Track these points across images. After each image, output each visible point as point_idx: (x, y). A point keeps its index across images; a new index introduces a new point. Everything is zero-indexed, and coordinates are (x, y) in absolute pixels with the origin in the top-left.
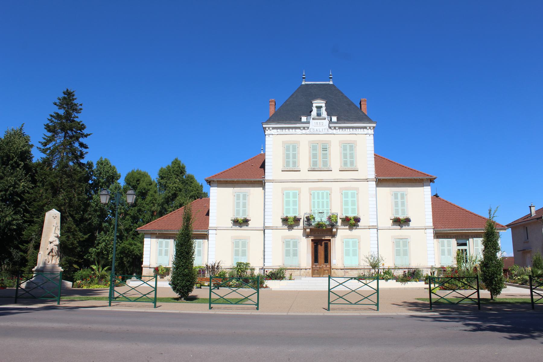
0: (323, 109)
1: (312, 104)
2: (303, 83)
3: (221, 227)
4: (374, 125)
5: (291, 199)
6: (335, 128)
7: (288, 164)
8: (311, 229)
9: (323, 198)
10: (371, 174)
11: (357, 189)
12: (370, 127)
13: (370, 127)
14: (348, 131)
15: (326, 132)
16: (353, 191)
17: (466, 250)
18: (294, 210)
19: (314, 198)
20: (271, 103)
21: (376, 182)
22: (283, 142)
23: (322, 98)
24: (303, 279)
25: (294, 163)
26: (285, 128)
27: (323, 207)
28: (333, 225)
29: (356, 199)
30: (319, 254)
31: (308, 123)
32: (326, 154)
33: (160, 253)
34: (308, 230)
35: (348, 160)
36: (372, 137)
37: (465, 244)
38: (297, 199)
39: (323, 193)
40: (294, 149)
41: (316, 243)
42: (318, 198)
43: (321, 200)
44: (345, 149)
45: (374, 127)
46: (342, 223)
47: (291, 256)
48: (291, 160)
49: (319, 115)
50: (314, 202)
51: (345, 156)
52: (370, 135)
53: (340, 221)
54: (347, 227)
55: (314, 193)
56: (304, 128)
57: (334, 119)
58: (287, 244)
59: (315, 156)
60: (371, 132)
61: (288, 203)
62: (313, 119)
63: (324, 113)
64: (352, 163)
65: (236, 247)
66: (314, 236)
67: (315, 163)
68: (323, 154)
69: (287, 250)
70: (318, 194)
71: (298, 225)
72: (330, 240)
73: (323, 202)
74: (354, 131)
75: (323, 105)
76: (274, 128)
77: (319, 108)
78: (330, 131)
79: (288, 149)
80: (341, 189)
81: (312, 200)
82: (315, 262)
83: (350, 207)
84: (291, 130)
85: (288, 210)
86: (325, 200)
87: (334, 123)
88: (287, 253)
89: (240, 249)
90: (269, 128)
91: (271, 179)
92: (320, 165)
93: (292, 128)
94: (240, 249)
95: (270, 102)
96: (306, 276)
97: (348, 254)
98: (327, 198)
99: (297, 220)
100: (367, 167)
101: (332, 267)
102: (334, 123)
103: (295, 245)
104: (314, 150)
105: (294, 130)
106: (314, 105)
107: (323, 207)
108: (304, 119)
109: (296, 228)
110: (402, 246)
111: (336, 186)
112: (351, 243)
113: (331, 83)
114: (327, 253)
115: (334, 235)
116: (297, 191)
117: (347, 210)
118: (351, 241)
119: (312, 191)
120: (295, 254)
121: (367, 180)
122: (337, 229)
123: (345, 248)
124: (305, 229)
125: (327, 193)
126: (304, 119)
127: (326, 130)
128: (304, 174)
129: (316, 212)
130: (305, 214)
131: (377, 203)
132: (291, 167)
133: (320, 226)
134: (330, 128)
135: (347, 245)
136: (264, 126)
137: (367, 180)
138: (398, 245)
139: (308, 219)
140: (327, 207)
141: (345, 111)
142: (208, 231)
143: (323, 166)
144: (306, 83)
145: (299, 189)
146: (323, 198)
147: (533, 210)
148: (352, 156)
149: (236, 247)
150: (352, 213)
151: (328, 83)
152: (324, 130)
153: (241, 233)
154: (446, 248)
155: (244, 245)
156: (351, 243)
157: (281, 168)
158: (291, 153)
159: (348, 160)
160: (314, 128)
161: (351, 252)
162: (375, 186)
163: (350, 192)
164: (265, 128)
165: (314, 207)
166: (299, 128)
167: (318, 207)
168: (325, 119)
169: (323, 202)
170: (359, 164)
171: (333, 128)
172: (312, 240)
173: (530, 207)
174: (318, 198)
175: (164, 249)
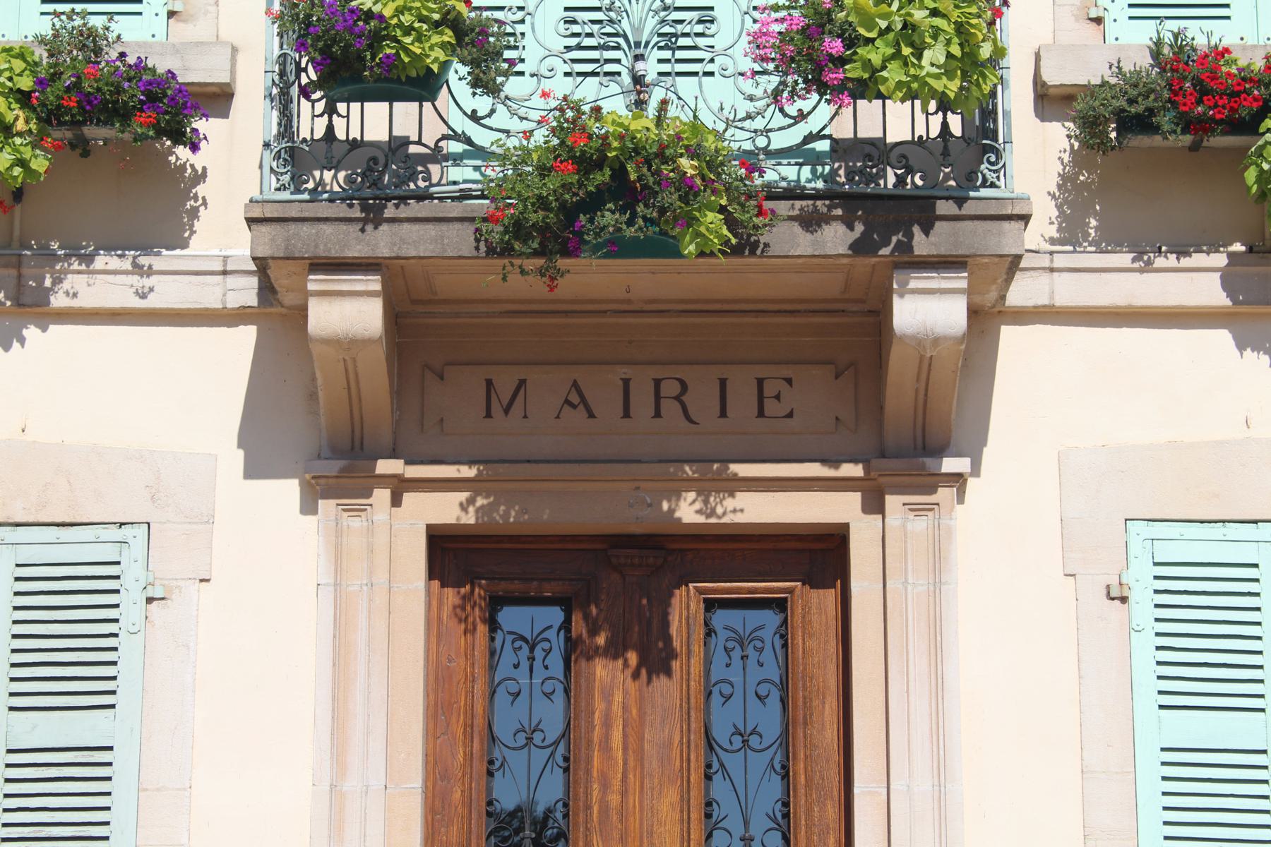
28: (902, 205)
34: (349, 313)
46: (1074, 197)
53: (1035, 157)
54: (1199, 281)
66: (497, 468)
71: (159, 218)
72: (823, 555)
109: (102, 282)
115: (911, 435)
122: (986, 317)
124: (276, 304)
133: (606, 188)
172: (448, 553)
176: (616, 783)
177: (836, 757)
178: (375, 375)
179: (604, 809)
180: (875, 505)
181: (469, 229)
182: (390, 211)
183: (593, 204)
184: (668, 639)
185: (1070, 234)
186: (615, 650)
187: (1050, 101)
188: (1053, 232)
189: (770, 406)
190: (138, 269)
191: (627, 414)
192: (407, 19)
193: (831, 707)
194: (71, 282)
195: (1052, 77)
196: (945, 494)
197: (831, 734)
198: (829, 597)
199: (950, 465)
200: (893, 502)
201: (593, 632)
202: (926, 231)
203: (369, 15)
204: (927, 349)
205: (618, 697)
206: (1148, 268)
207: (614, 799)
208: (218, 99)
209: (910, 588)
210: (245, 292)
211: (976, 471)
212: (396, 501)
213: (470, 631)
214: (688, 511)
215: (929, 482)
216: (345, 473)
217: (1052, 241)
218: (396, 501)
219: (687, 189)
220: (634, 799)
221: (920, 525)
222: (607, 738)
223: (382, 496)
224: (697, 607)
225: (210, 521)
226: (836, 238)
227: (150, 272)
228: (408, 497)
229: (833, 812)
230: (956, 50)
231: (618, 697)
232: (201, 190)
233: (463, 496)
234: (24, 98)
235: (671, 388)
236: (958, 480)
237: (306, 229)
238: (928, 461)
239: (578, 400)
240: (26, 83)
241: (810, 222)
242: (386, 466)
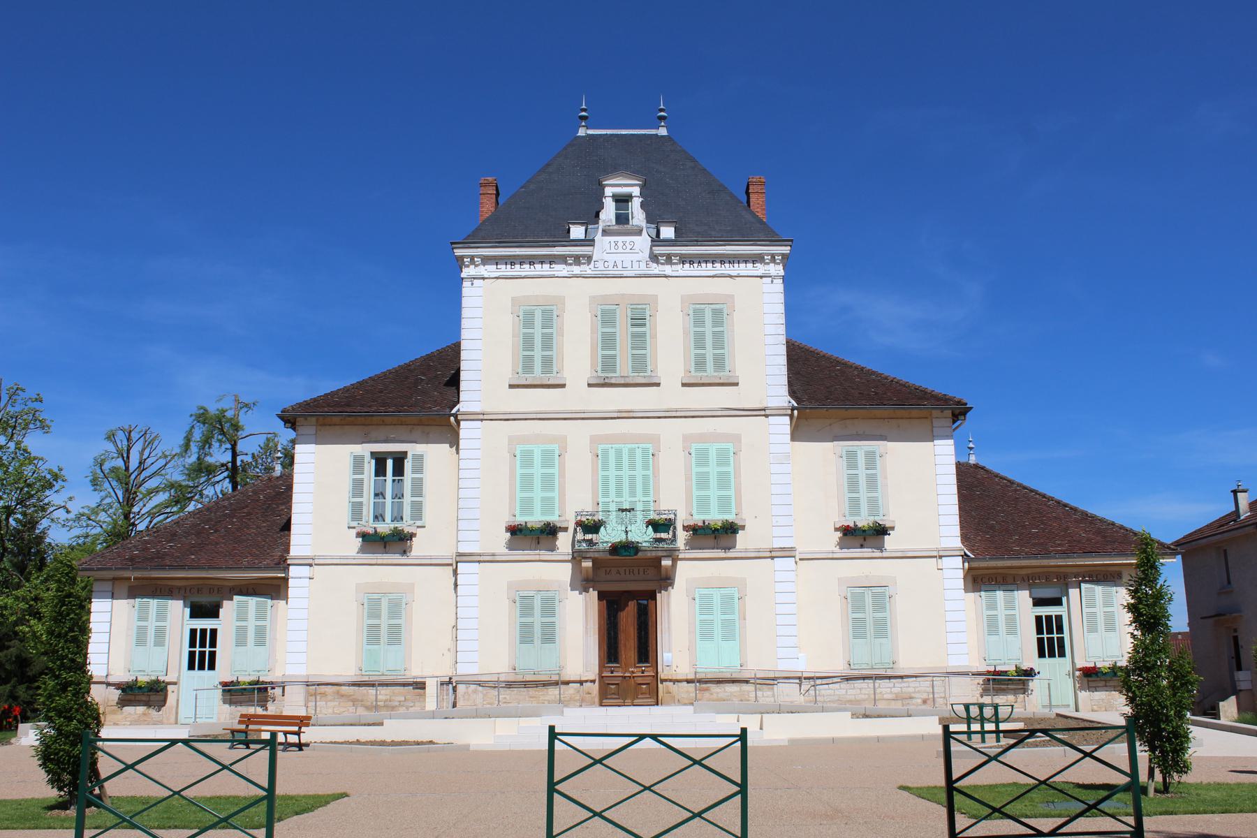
0: (636, 203)
1: (602, 187)
2: (582, 132)
3: (324, 557)
4: (786, 250)
5: (537, 471)
6: (669, 259)
7: (528, 364)
8: (595, 561)
9: (632, 466)
10: (780, 396)
11: (736, 439)
12: (773, 256)
13: (773, 256)
14: (707, 269)
15: (643, 269)
16: (724, 446)
17: (1059, 618)
18: (547, 504)
19: (605, 467)
20: (483, 190)
21: (791, 416)
22: (513, 299)
23: (632, 172)
25: (547, 363)
26: (522, 260)
27: (633, 493)
29: (731, 469)
30: (622, 637)
31: (588, 242)
32: (643, 335)
33: (141, 640)
35: (709, 352)
36: (779, 286)
37: (1057, 602)
38: (556, 471)
39: (632, 453)
40: (548, 319)
41: (612, 605)
42: (619, 467)
43: (626, 473)
44: (699, 320)
45: (783, 255)
47: (537, 641)
48: (538, 354)
49: (622, 219)
50: (606, 479)
51: (699, 341)
52: (772, 277)
53: (682, 537)
55: (606, 452)
56: (577, 260)
57: (668, 232)
58: (525, 605)
59: (608, 341)
60: (777, 270)
61: (527, 482)
62: (605, 232)
63: (637, 215)
64: (720, 362)
65: (370, 616)
67: (609, 363)
68: (634, 335)
69: (523, 625)
70: (619, 453)
73: (632, 478)
74: (727, 269)
75: (636, 191)
76: (486, 260)
77: (623, 200)
78: (655, 269)
79: (528, 321)
80: (687, 439)
81: (601, 473)
82: (610, 661)
83: (714, 493)
84: (538, 266)
85: (527, 505)
86: (639, 472)
87: (668, 242)
88: (526, 635)
89: (384, 622)
90: (472, 258)
91: (478, 410)
92: (624, 368)
93: (542, 260)
94: (384, 622)
95: (481, 185)
96: (582, 703)
97: (707, 635)
98: (646, 467)
99: (550, 531)
100: (765, 375)
101: (662, 675)
102: (668, 242)
103: (549, 608)
104: (604, 323)
105: (546, 266)
106: (609, 191)
107: (633, 493)
108: (577, 232)
110: (869, 611)
111: (671, 431)
112: (717, 600)
113: (663, 132)
114: (647, 633)
116: (555, 447)
117: (704, 503)
118: (717, 596)
119: (601, 447)
120: (549, 636)
121: (763, 412)
122: (675, 560)
123: (699, 618)
125: (645, 451)
126: (577, 232)
127: (643, 265)
128: (577, 395)
129: (613, 507)
130: (577, 514)
131: (793, 482)
132: (537, 375)
133: (624, 549)
134: (654, 258)
135: (706, 607)
136: (458, 252)
137: (763, 412)
138: (858, 605)
140: (646, 493)
141: (700, 214)
142: (286, 568)
143: (635, 370)
144: (591, 132)
145: (562, 441)
146: (632, 466)
147: (1244, 500)
148: (719, 340)
149: (370, 616)
150: (720, 512)
151: (653, 132)
152: (636, 265)
153: (386, 573)
154: (1001, 612)
155: (396, 609)
156: (717, 600)
157: (508, 376)
158: (538, 332)
159: (709, 352)
160: (606, 257)
161: (718, 630)
162: (788, 429)
163: (713, 449)
164: (462, 257)
165: (606, 494)
166: (563, 259)
167: (619, 493)
168: (639, 232)
169: (632, 478)
170: (740, 365)
171: (662, 259)
173: (1235, 492)
174: (619, 467)
175: (152, 624)
178: (591, 571)
187: (686, 528)
204: (666, 568)
239: (618, 572)
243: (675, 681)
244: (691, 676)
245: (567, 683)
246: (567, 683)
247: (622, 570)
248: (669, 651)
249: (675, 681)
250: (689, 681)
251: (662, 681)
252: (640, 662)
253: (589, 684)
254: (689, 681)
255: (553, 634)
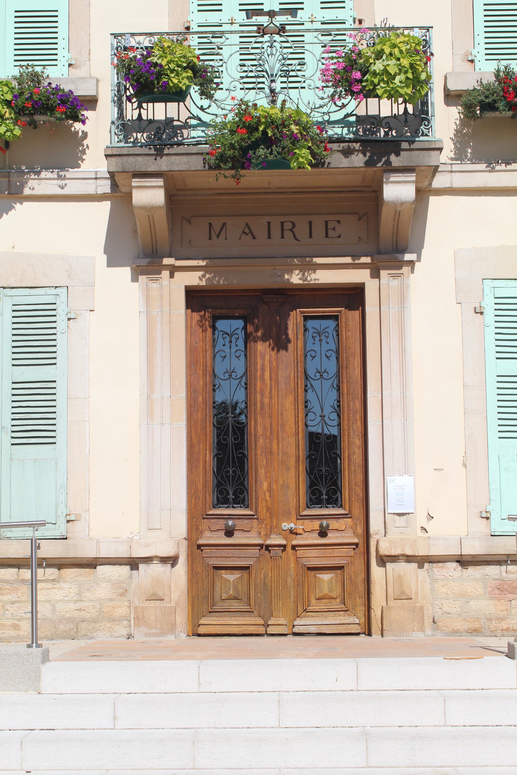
24: (63, 675)
28: (386, 144)
34: (150, 195)
46: (461, 139)
53: (445, 122)
66: (215, 261)
72: (353, 297)
82: (222, 500)
101: (384, 543)
115: (392, 245)
122: (423, 193)
124: (119, 193)
133: (258, 140)
139: (145, 77)
172: (194, 297)
176: (267, 393)
177: (360, 381)
178: (162, 221)
179: (262, 404)
180: (376, 275)
181: (200, 158)
182: (166, 151)
183: (255, 146)
184: (287, 335)
185: (460, 156)
186: (264, 339)
187: (451, 97)
188: (452, 155)
189: (331, 233)
190: (60, 177)
191: (269, 237)
192: (172, 66)
193: (357, 362)
194: (31, 183)
195: (453, 86)
196: (405, 269)
197: (357, 372)
198: (356, 314)
199: (408, 257)
200: (384, 273)
201: (257, 331)
202: (398, 155)
203: (156, 65)
204: (398, 207)
205: (267, 358)
206: (493, 170)
207: (266, 400)
208: (91, 102)
209: (391, 310)
210: (105, 187)
211: (419, 259)
212: (172, 276)
213: (204, 331)
214: (296, 279)
215: (399, 264)
216: (150, 264)
217: (452, 159)
218: (172, 276)
219: (294, 139)
220: (274, 400)
221: (395, 283)
222: (263, 375)
223: (166, 274)
224: (300, 319)
225: (93, 285)
226: (358, 160)
227: (65, 178)
228: (177, 274)
229: (358, 404)
230: (410, 75)
231: (267, 358)
232: (85, 142)
233: (200, 273)
234: (8, 103)
235: (288, 226)
236: (411, 263)
237: (131, 159)
238: (399, 256)
239: (248, 231)
240: (9, 97)
241: (347, 153)
242: (167, 261)
243: (422, 561)
244: (471, 549)
245: (92, 564)
246: (92, 564)
247: (259, 225)
248: (406, 470)
249: (422, 561)
250: (464, 562)
251: (383, 561)
252: (315, 498)
253: (157, 568)
254: (464, 562)
255: (50, 418)
